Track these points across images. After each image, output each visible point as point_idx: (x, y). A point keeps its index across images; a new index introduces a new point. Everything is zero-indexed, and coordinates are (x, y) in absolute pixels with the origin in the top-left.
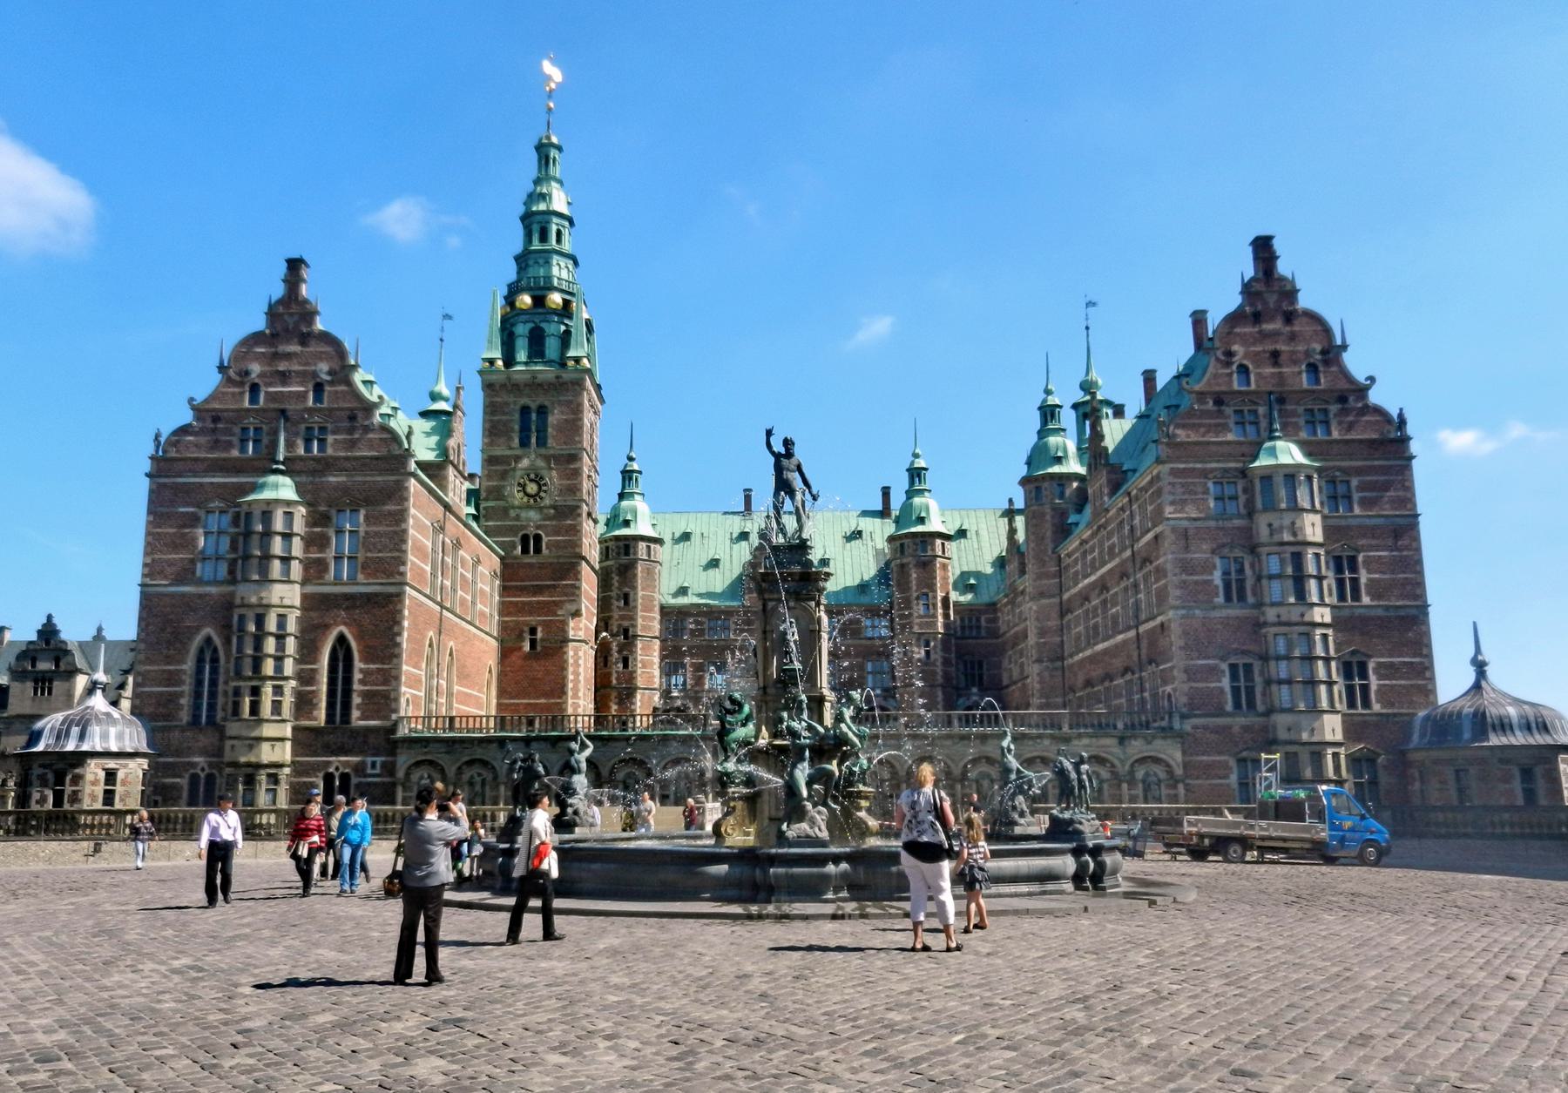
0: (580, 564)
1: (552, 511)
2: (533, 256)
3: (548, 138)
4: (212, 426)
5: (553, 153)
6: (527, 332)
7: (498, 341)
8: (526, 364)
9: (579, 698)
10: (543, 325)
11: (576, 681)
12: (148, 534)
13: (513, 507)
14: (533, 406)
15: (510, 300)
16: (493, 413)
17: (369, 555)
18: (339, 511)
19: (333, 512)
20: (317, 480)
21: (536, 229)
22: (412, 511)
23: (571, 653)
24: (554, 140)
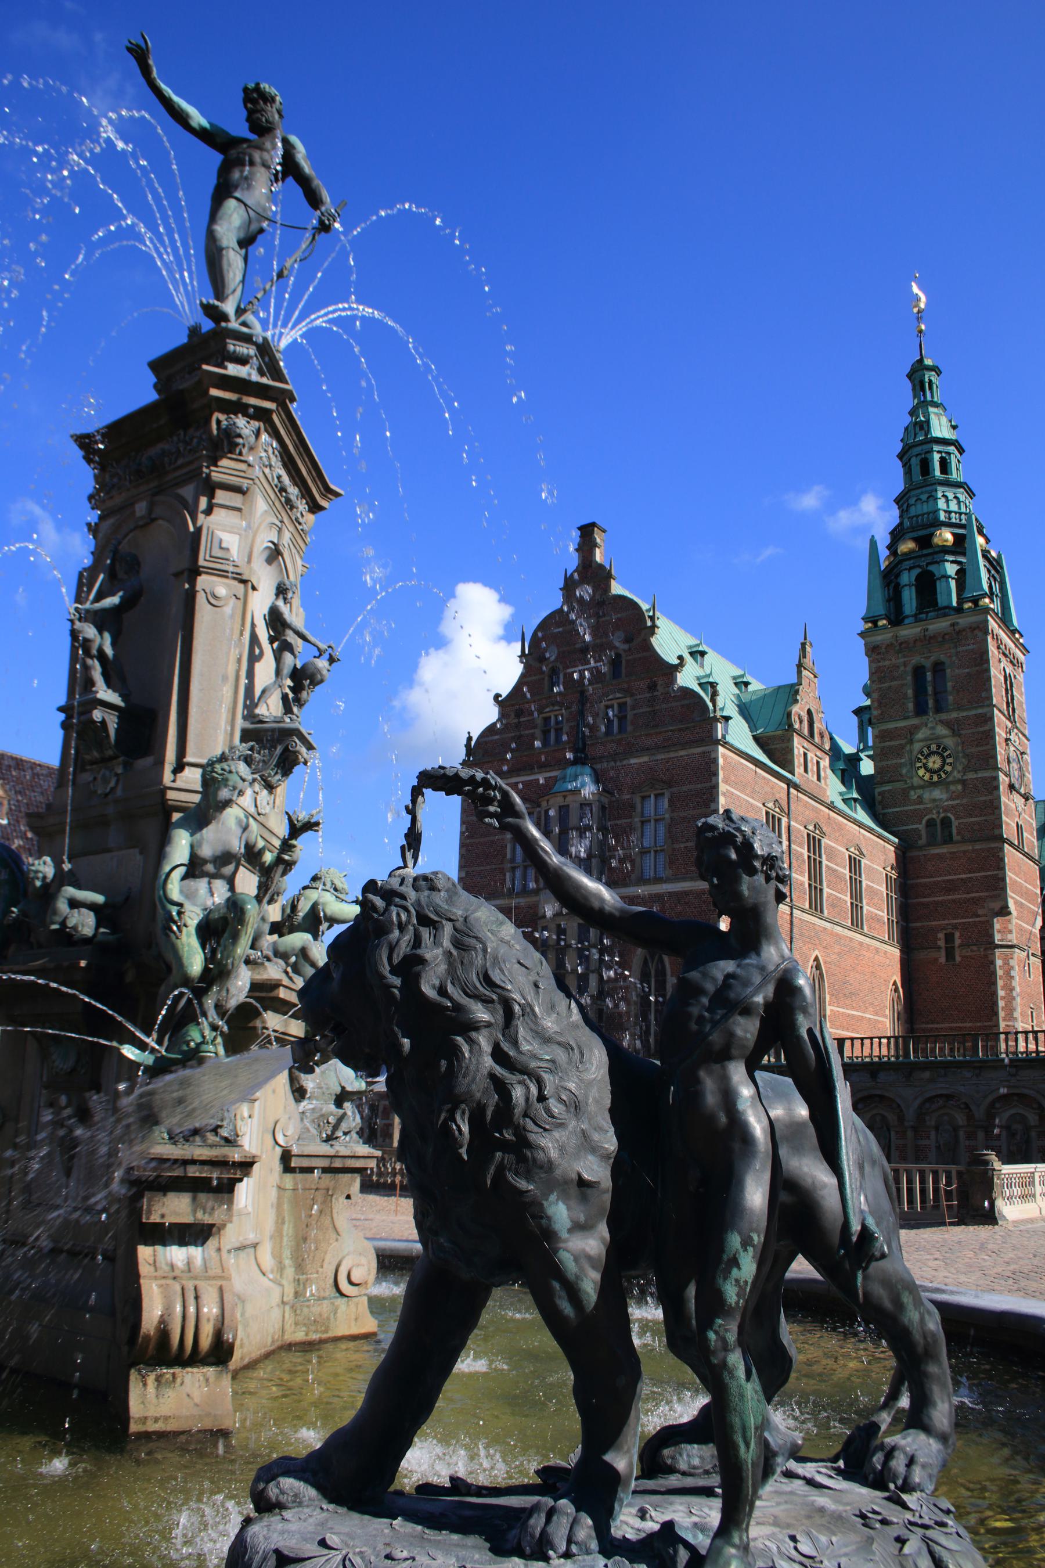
0: (1002, 849)
1: (960, 787)
2: (913, 493)
3: (921, 361)
4: (516, 721)
5: (929, 376)
6: (913, 579)
7: (879, 596)
8: (915, 616)
9: (1016, 1019)
10: (931, 568)
11: (1010, 998)
12: (462, 845)
13: (913, 788)
14: (928, 664)
15: (892, 547)
16: (881, 680)
17: (676, 846)
18: (643, 798)
19: (637, 800)
20: (618, 764)
21: (915, 462)
22: (723, 787)
23: (999, 962)
24: (928, 362)
